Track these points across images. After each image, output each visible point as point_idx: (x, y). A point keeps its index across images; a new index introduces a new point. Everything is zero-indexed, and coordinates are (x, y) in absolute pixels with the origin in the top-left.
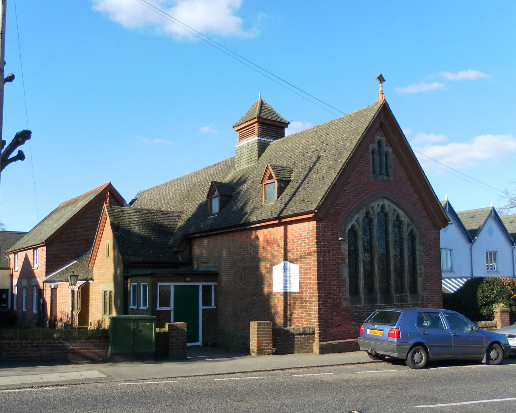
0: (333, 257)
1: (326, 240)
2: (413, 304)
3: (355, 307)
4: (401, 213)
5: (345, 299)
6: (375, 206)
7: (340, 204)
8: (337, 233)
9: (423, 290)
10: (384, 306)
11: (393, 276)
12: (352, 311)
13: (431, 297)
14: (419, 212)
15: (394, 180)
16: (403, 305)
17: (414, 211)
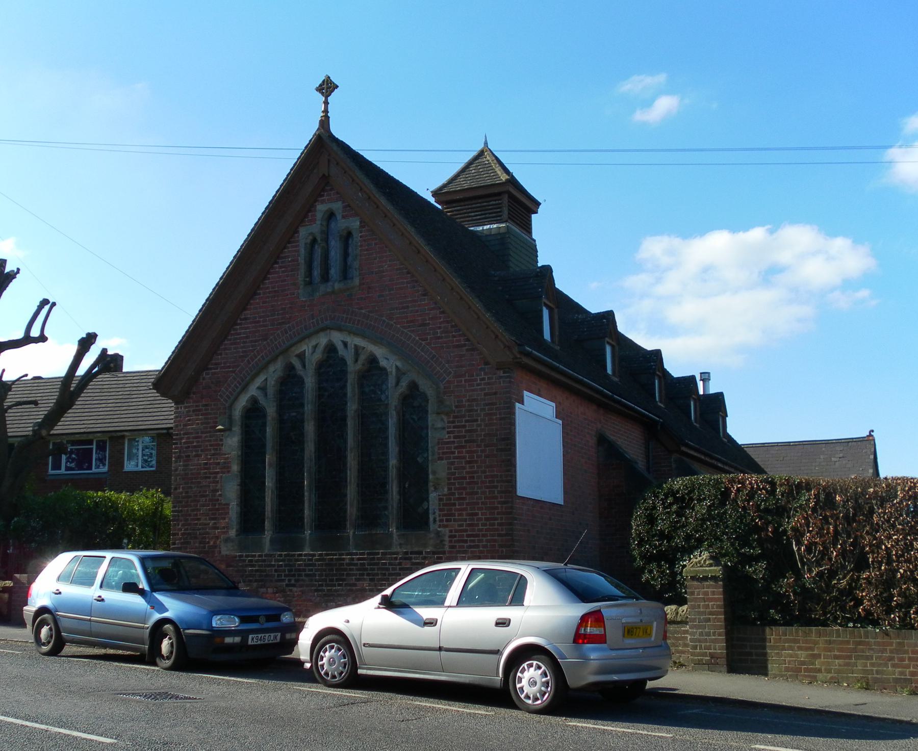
0: (206, 464)
1: (192, 433)
2: (406, 553)
3: (247, 556)
4: (379, 352)
5: (227, 540)
6: (307, 351)
7: (225, 363)
8: (216, 418)
9: (441, 521)
10: (321, 555)
11: (351, 491)
12: (240, 564)
13: (468, 536)
14: (439, 338)
15: (361, 284)
16: (378, 554)
17: (419, 339)
